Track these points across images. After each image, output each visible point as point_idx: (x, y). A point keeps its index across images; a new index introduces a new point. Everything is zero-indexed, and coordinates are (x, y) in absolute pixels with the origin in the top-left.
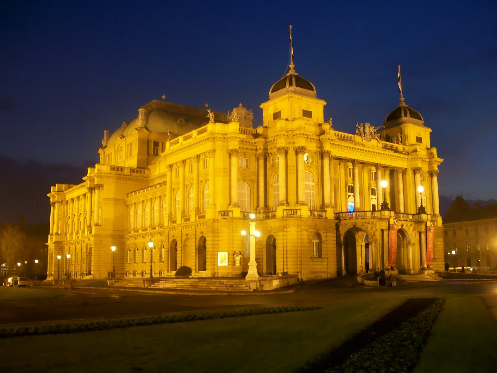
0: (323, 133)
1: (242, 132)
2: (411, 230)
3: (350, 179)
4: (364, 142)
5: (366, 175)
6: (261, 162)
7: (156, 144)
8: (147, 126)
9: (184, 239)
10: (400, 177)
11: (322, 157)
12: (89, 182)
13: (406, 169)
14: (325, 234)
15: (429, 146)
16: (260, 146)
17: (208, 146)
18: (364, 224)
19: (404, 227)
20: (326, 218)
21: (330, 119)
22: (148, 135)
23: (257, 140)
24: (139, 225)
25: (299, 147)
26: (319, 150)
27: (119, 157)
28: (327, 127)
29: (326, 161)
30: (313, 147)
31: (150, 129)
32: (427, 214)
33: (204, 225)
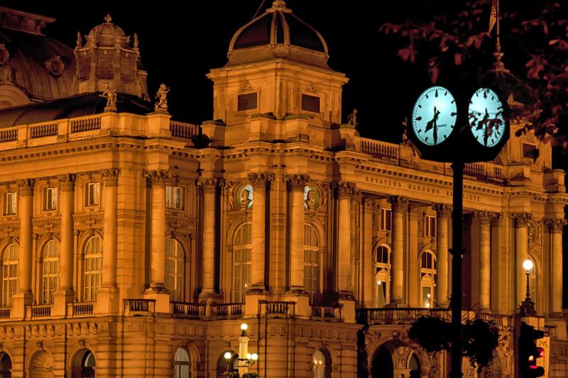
0: (340, 145)
1: (176, 133)
3: (382, 233)
5: (414, 225)
6: (210, 198)
9: (30, 353)
10: (486, 232)
11: (336, 196)
13: (498, 215)
15: (549, 165)
16: (207, 167)
17: (103, 161)
20: (341, 321)
21: (352, 113)
23: (202, 152)
25: (296, 176)
26: (331, 180)
28: (348, 132)
29: (345, 204)
30: (320, 173)
32: (539, 317)
33: (80, 327)
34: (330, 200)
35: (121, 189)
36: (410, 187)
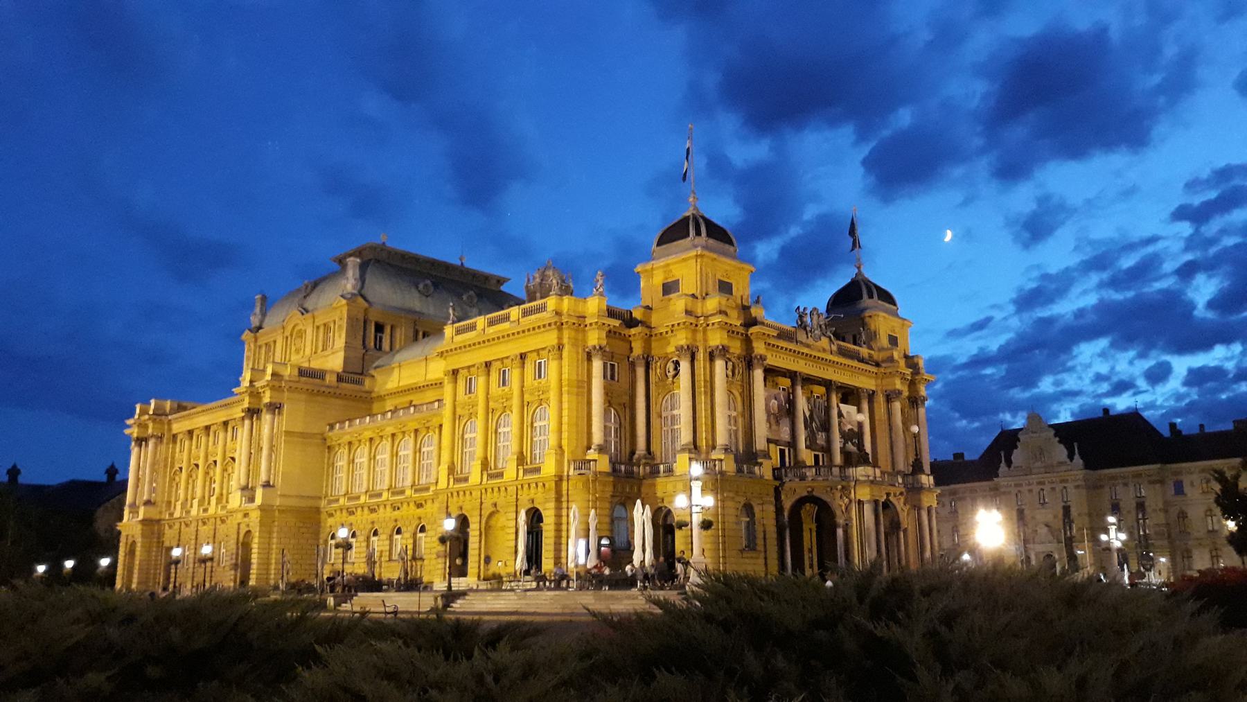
2: (902, 505)
4: (810, 341)
6: (640, 372)
7: (379, 328)
8: (363, 292)
9: (486, 513)
12: (247, 400)
13: (874, 392)
14: (760, 507)
17: (550, 338)
18: (829, 489)
19: (891, 498)
20: (762, 477)
22: (366, 310)
23: (633, 331)
24: (361, 486)
25: (718, 347)
26: (744, 353)
27: (293, 348)
31: (370, 298)
34: (744, 371)
35: (565, 362)
36: (806, 364)
